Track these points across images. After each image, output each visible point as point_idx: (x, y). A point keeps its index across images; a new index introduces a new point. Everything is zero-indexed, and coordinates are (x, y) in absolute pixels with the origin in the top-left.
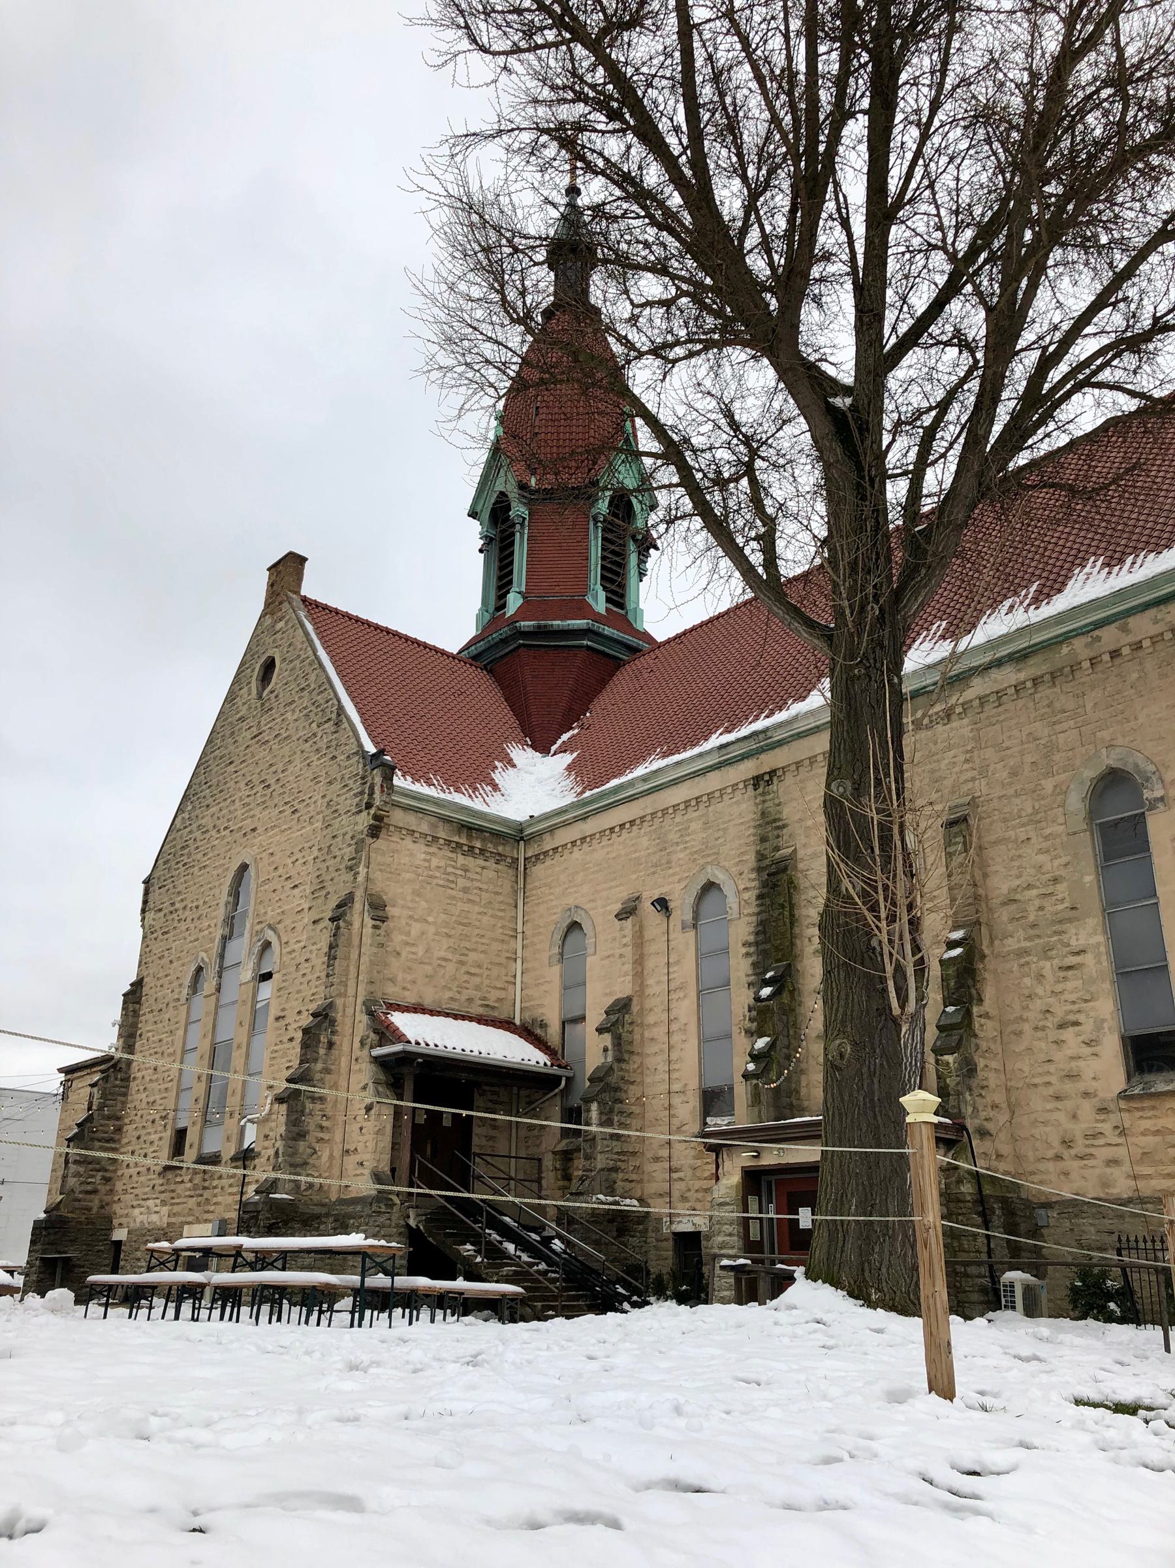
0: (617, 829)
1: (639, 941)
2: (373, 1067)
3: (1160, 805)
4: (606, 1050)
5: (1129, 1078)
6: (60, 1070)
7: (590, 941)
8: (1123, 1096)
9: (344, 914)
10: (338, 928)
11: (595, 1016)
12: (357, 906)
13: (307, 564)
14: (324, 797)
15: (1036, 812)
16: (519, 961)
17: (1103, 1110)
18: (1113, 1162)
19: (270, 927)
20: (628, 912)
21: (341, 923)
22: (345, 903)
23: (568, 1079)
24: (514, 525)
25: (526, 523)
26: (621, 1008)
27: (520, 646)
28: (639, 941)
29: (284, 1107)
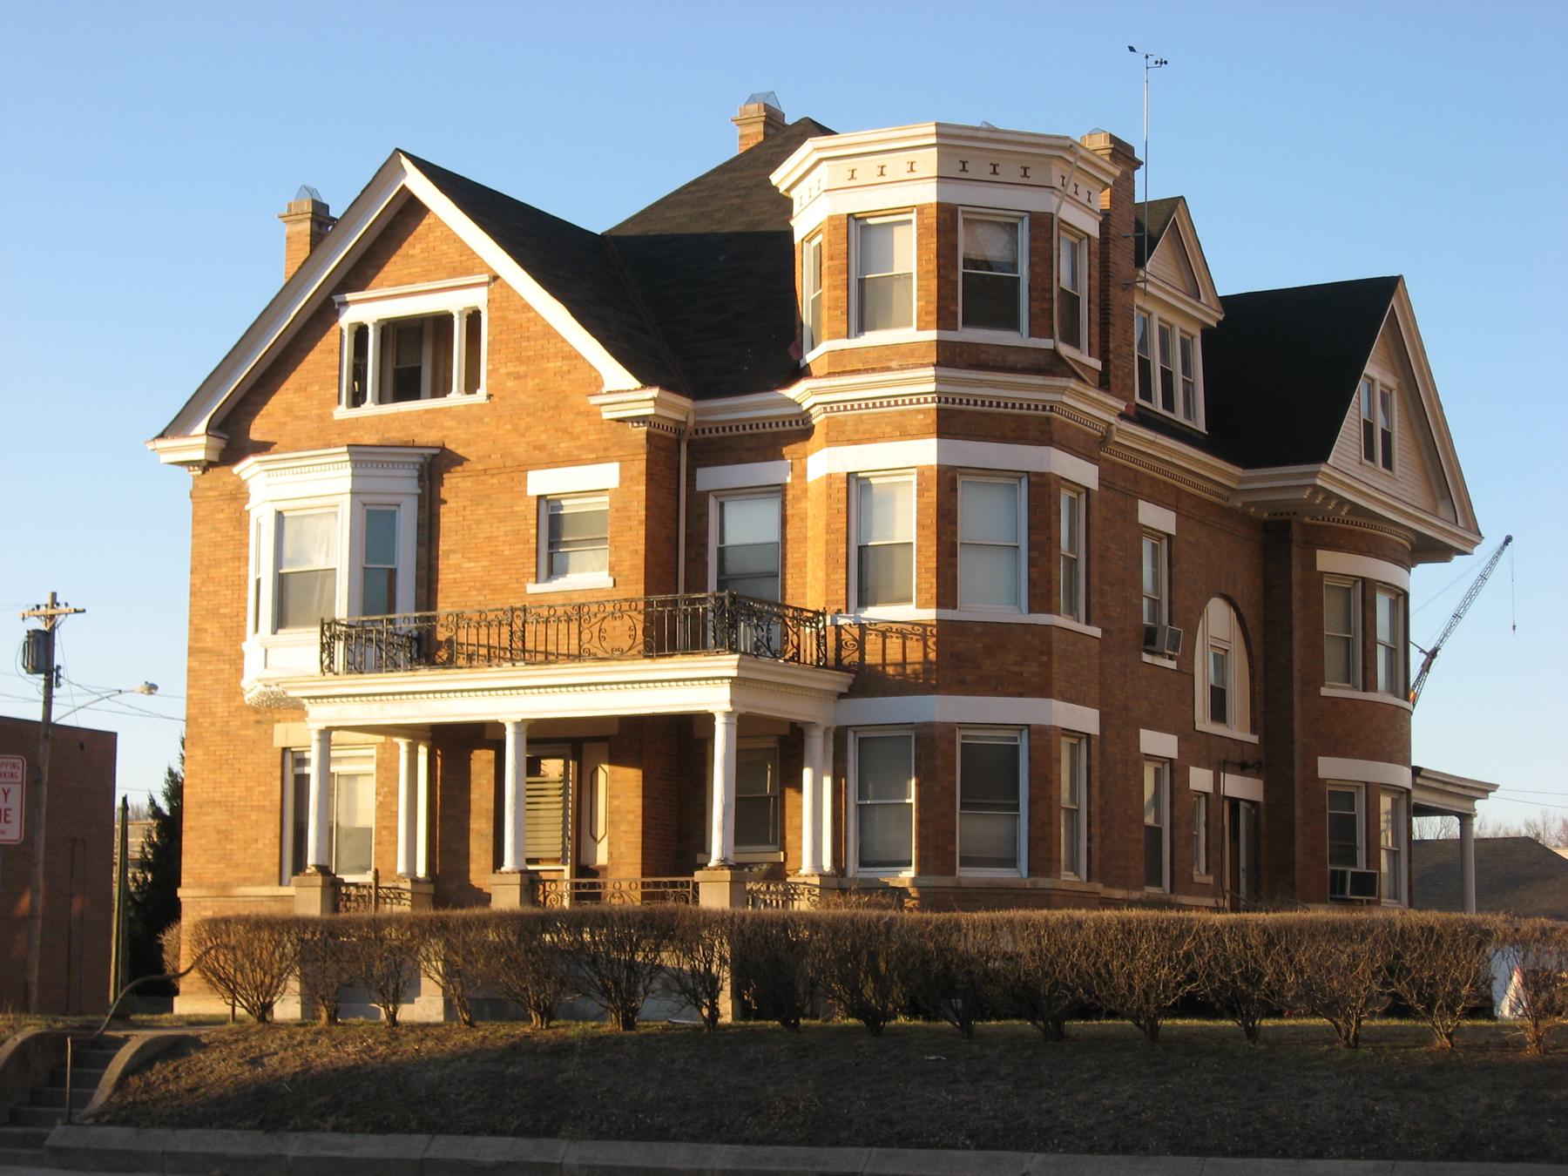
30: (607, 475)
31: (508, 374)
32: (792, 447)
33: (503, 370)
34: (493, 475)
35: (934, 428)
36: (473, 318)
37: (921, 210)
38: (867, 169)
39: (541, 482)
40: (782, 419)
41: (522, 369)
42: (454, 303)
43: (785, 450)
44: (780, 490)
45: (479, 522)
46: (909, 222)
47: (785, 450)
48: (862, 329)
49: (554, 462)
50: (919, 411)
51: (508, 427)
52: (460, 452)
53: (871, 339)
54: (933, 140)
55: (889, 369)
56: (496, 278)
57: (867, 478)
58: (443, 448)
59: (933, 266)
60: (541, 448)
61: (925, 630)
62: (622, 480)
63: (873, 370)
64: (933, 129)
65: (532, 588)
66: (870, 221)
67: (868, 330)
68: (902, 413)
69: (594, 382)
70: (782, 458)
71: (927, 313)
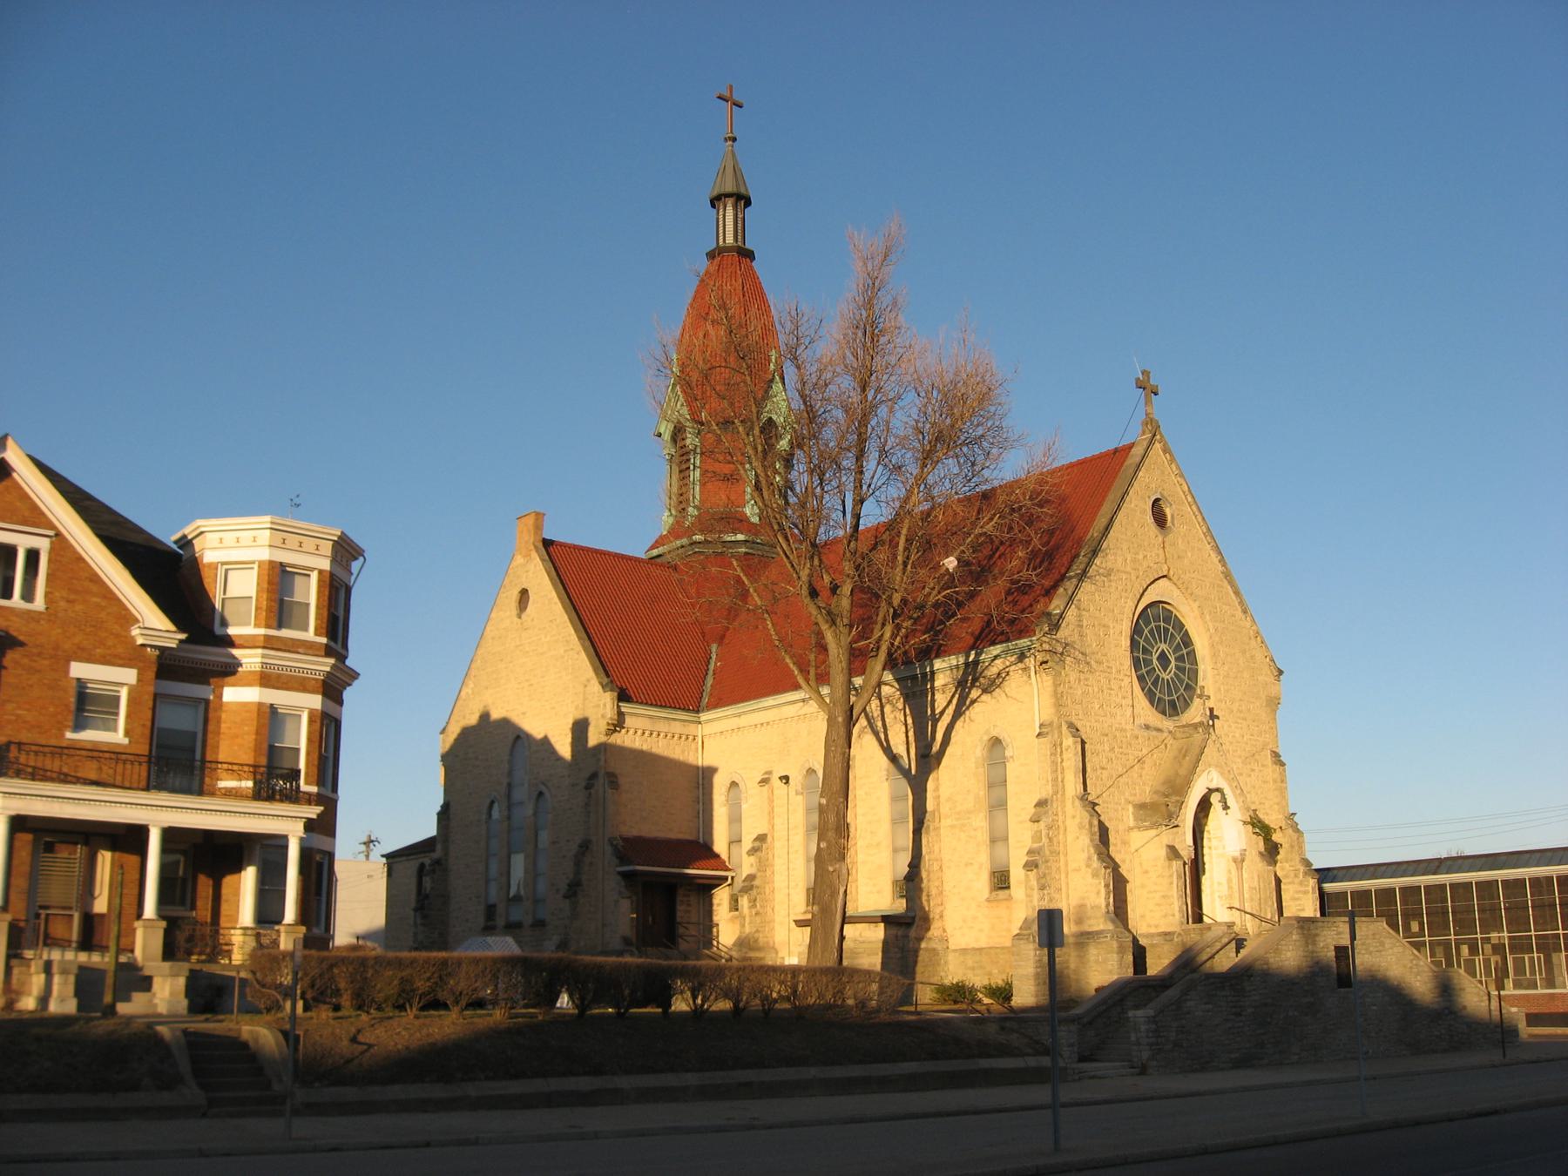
0: (759, 726)
1: (771, 801)
2: (619, 878)
3: (1011, 760)
4: (752, 865)
5: (991, 891)
6: (383, 856)
7: (743, 796)
8: (988, 900)
9: (593, 785)
10: (590, 794)
11: (747, 843)
12: (601, 780)
13: (545, 518)
14: (572, 702)
15: (963, 755)
16: (701, 804)
17: (979, 906)
18: (981, 930)
19: (543, 784)
20: (764, 781)
21: (592, 791)
22: (594, 776)
23: (733, 878)
24: (689, 453)
25: (698, 450)
26: (761, 838)
27: (696, 552)
28: (771, 801)
29: (567, 901)
30: (129, 675)
31: (62, 598)
32: (215, 680)
33: (57, 594)
34: (45, 658)
35: (321, 690)
36: (33, 556)
37: (321, 572)
38: (293, 541)
39: (78, 670)
40: (214, 663)
41: (72, 597)
42: (23, 542)
43: (211, 680)
44: (207, 702)
45: (31, 686)
46: (252, 568)
47: (211, 680)
48: (280, 626)
49: (90, 659)
50: (314, 679)
51: (59, 631)
52: (21, 638)
53: (285, 633)
54: (336, 539)
55: (298, 653)
56: (58, 534)
57: (277, 708)
58: (7, 633)
59: (326, 603)
60: (83, 649)
61: (310, 798)
62: (139, 680)
63: (289, 651)
64: (339, 534)
65: (69, 735)
66: (288, 569)
67: (285, 628)
68: (304, 678)
69: (127, 618)
70: (209, 684)
71: (322, 628)
